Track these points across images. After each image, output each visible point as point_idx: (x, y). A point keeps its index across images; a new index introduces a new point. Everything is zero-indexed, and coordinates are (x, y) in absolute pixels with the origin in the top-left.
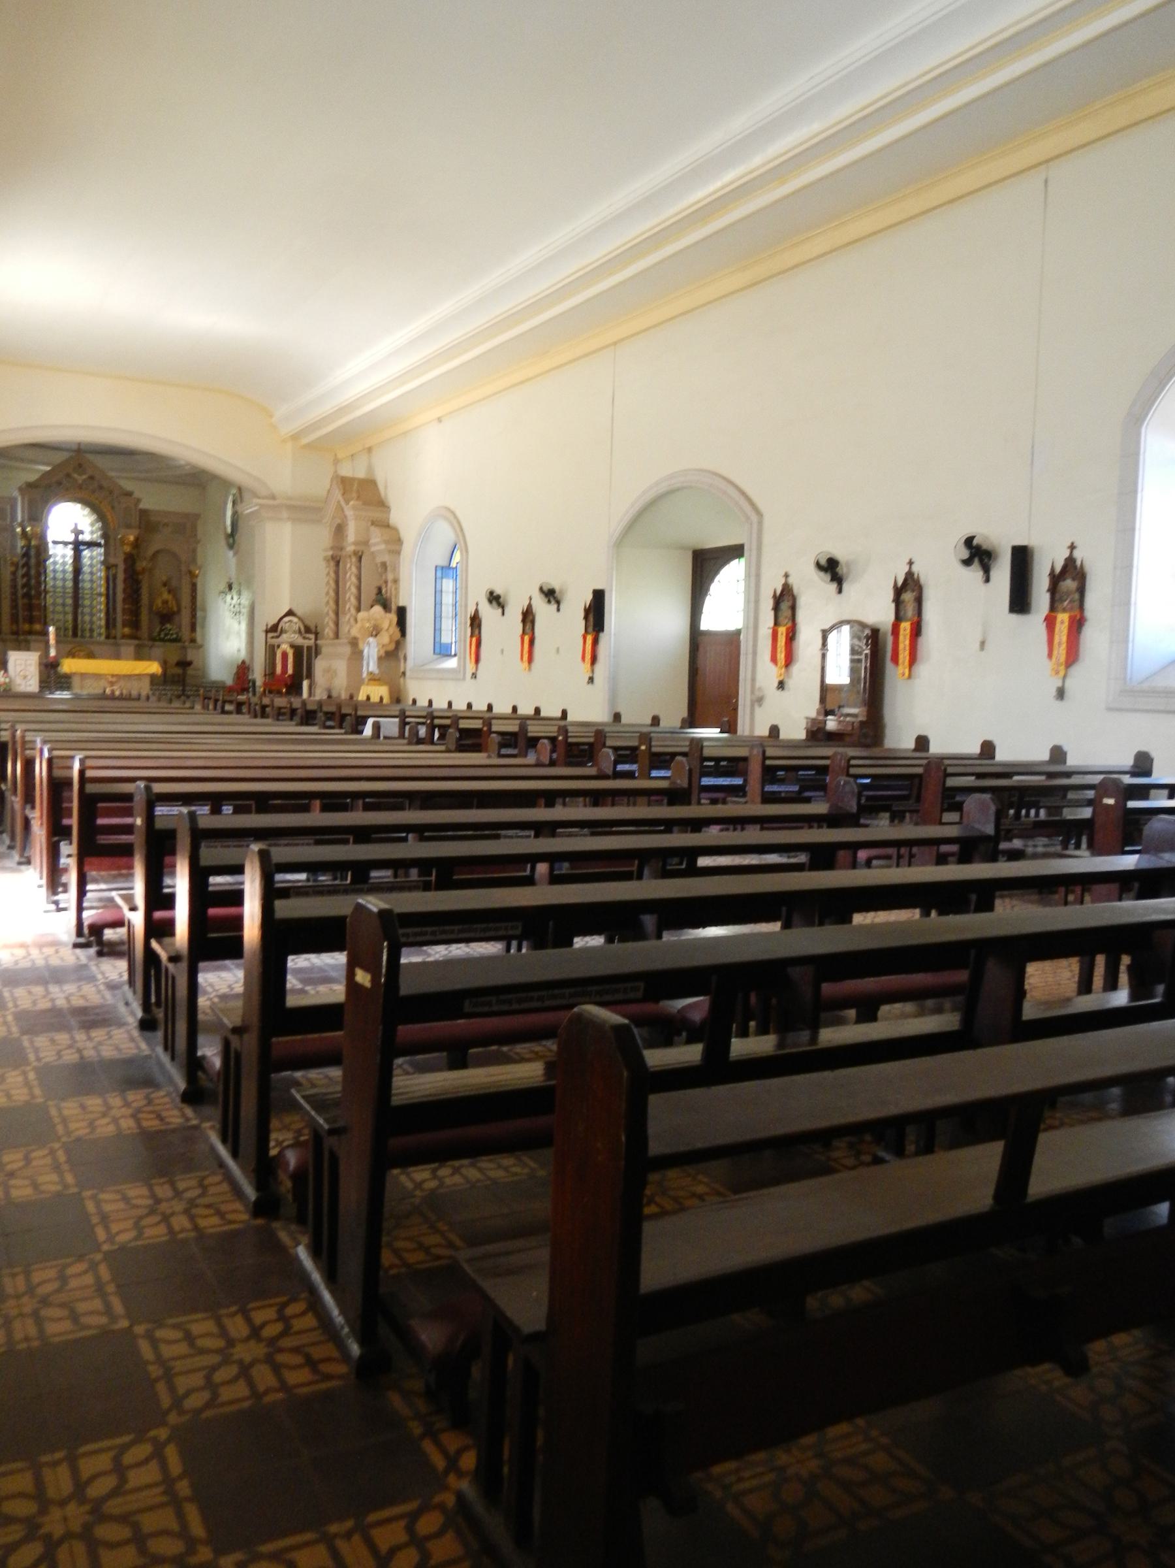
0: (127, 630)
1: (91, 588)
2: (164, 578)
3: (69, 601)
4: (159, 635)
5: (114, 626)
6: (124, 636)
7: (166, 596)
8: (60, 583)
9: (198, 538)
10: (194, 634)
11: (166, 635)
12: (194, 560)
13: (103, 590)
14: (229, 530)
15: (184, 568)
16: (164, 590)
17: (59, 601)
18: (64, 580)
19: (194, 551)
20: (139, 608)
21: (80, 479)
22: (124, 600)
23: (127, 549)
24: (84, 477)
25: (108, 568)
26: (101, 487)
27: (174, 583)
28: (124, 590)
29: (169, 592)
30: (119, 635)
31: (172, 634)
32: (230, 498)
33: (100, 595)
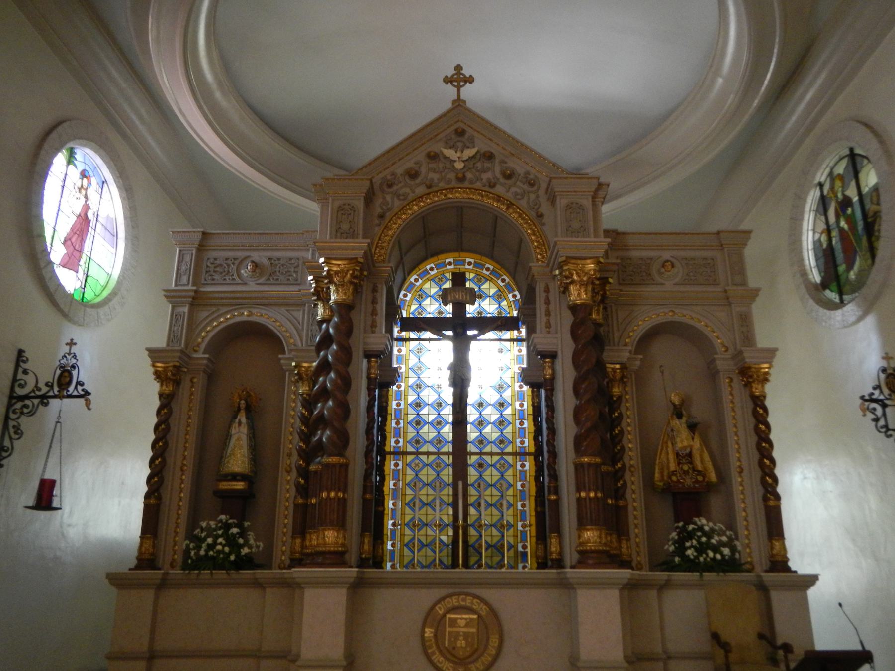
0: (590, 535)
1: (502, 441)
3: (447, 474)
4: (681, 549)
5: (557, 529)
6: (585, 558)
7: (684, 439)
8: (429, 433)
9: (752, 283)
11: (701, 549)
12: (748, 339)
13: (528, 444)
14: (816, 277)
15: (724, 364)
17: (427, 475)
18: (438, 423)
19: (746, 320)
20: (618, 475)
21: (457, 157)
22: (578, 443)
23: (578, 295)
24: (469, 153)
25: (535, 386)
26: (509, 176)
27: (700, 411)
28: (577, 413)
29: (692, 427)
30: (570, 556)
32: (813, 196)
33: (521, 454)
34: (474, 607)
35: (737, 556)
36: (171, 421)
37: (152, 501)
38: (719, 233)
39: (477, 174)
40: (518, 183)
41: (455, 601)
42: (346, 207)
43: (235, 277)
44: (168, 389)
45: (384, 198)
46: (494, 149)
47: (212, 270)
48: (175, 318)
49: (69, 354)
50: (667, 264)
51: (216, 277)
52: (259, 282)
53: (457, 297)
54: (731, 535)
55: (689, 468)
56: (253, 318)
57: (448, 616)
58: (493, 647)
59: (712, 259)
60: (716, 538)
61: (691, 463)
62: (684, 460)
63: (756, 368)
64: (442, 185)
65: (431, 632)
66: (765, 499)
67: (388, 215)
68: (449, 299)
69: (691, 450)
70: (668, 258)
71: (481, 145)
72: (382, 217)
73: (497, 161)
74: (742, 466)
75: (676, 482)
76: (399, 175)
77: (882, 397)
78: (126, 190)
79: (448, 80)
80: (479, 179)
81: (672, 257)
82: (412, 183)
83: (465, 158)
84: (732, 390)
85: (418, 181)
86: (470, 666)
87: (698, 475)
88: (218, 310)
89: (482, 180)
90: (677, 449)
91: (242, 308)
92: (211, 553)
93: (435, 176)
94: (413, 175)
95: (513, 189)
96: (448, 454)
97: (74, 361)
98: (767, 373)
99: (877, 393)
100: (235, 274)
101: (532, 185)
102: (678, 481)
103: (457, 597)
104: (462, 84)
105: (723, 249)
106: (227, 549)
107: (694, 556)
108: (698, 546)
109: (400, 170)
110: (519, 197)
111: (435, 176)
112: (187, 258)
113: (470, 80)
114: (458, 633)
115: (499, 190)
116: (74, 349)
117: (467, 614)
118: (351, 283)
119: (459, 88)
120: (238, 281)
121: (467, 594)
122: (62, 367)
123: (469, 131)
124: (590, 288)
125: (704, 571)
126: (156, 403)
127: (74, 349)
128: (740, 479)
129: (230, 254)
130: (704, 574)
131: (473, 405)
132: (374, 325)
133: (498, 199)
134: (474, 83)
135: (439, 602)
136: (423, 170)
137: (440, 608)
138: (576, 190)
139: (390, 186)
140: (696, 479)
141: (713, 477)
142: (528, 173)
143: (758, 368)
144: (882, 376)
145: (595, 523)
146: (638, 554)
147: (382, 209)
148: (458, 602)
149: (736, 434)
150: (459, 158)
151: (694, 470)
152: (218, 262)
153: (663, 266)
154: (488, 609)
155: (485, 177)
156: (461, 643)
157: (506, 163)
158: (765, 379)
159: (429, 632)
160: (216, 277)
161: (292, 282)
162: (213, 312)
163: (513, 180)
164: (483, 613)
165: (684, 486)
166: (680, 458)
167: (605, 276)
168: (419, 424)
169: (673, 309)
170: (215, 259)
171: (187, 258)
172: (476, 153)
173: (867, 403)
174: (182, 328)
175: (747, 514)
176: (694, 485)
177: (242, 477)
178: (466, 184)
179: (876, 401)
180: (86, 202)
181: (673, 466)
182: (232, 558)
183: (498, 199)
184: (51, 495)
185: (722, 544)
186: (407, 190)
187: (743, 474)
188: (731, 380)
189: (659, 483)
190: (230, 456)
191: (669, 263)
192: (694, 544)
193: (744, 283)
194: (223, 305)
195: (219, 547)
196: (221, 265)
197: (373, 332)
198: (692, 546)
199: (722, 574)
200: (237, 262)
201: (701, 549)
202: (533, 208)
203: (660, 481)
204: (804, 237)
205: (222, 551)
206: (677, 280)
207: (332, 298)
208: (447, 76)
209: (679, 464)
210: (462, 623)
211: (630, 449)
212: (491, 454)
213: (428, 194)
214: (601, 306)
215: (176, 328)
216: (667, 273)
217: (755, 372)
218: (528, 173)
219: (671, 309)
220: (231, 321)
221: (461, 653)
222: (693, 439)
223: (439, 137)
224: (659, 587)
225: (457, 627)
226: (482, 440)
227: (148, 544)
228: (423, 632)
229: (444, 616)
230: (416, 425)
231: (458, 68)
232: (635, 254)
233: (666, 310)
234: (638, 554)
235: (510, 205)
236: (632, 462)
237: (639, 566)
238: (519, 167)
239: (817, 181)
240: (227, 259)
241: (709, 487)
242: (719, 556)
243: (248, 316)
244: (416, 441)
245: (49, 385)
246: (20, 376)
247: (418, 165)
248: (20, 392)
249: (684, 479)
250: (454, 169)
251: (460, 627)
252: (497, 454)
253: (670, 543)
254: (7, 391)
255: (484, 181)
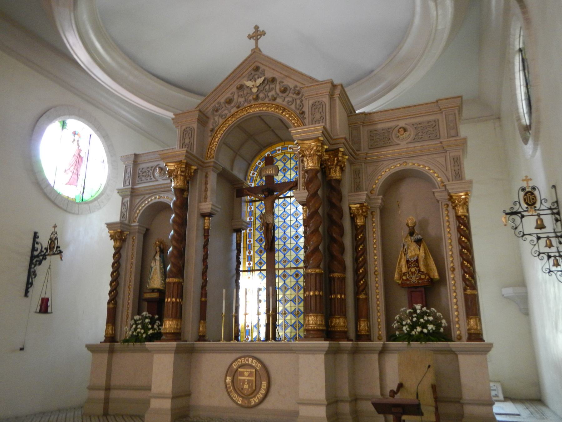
2: (411, 220)
7: (414, 251)
10: (472, 322)
11: (413, 326)
12: (459, 175)
14: (526, 120)
16: (410, 241)
24: (259, 81)
26: (284, 90)
27: (432, 231)
29: (418, 242)
31: (424, 326)
34: (253, 364)
35: (442, 330)
36: (120, 261)
37: (111, 306)
38: (437, 101)
39: (266, 93)
40: (290, 95)
41: (242, 361)
42: (188, 129)
43: (152, 177)
44: (118, 244)
45: (214, 119)
46: (276, 75)
47: (141, 175)
48: (123, 204)
49: (54, 232)
50: (400, 130)
51: (143, 179)
52: (164, 178)
53: (267, 172)
54: (440, 316)
55: (416, 270)
56: (162, 200)
57: (239, 370)
58: (264, 389)
59: (435, 121)
60: (426, 318)
61: (418, 266)
62: (412, 265)
63: (457, 196)
64: (246, 104)
65: (230, 379)
66: (465, 290)
67: (216, 129)
68: (263, 174)
69: (418, 257)
70: (403, 125)
71: (269, 74)
72: (212, 130)
73: (278, 83)
74: (454, 267)
75: (406, 280)
76: (222, 103)
77: (520, 210)
78: (104, 137)
79: (250, 37)
80: (267, 96)
81: (405, 124)
82: (229, 107)
83: (258, 85)
84: (448, 213)
85: (233, 105)
86: (251, 400)
87: (422, 274)
88: (144, 197)
89: (268, 97)
90: (408, 257)
91: (155, 195)
92: (135, 333)
93: (241, 100)
94: (229, 101)
95: (287, 99)
96: (279, 269)
97: (56, 235)
98: (465, 199)
99: (516, 208)
100: (152, 176)
101: (298, 94)
102: (407, 280)
103: (244, 358)
104: (259, 37)
105: (442, 113)
106: (142, 331)
107: (407, 331)
108: (411, 324)
109: (223, 101)
110: (290, 103)
111: (241, 100)
112: (129, 170)
113: (264, 33)
114: (244, 380)
115: (279, 101)
116: (56, 229)
117: (250, 369)
118: (181, 175)
119: (257, 40)
120: (154, 179)
121: (249, 357)
122: (51, 239)
123: (262, 67)
124: (316, 158)
125: (412, 341)
126: (113, 251)
127: (56, 229)
128: (452, 276)
129: (150, 165)
130: (411, 343)
131: (301, 237)
132: (206, 198)
133: (277, 107)
134: (266, 35)
135: (234, 362)
136: (236, 97)
137: (235, 365)
138: (318, 93)
139: (217, 111)
140: (420, 277)
141: (436, 275)
142: (296, 86)
143: (459, 196)
144: (522, 194)
145: (316, 312)
146: (379, 329)
147: (213, 125)
148: (245, 361)
149: (451, 244)
150: (253, 85)
151: (419, 271)
152: (144, 170)
153: (399, 132)
154: (261, 366)
155: (270, 94)
156: (246, 386)
157: (283, 82)
158: (465, 203)
159: (229, 379)
160: (143, 179)
161: (149, 180)
162: (143, 198)
163: (287, 93)
164: (258, 368)
165: (411, 282)
166: (410, 263)
167: (338, 147)
168: (262, 252)
169: (406, 161)
170: (143, 169)
171: (129, 170)
172: (264, 80)
173: (508, 216)
174: (127, 209)
175: (457, 300)
176: (418, 282)
177: (159, 290)
178: (260, 101)
179: (516, 213)
180: (78, 148)
181: (404, 269)
182: (144, 336)
183: (277, 107)
184: (47, 307)
185: (428, 322)
186: (226, 112)
187: (455, 272)
188: (448, 205)
189: (398, 281)
190: (151, 279)
191: (402, 129)
192: (408, 323)
193: (457, 135)
194: (147, 194)
195: (139, 330)
196: (146, 172)
197: (206, 202)
198: (407, 324)
199: (423, 343)
200: (153, 169)
201: (413, 326)
202: (299, 109)
203: (400, 280)
204: (518, 92)
205: (140, 332)
206: (409, 140)
207: (173, 185)
208: (249, 35)
209: (408, 268)
210: (246, 374)
211: (376, 260)
212: (291, 268)
213: (237, 112)
214: (338, 168)
215: (124, 210)
216: (402, 136)
217: (456, 199)
218: (296, 86)
219: (404, 161)
220: (150, 203)
221: (246, 392)
222: (419, 249)
223: (244, 75)
224: (378, 352)
225: (243, 376)
226: (298, 260)
227: (110, 328)
228: (226, 379)
229: (237, 370)
230: (260, 253)
231: (256, 28)
232: (380, 126)
233: (401, 162)
234: (379, 329)
235: (284, 110)
236: (376, 268)
237: (380, 338)
238: (291, 84)
239: (517, 48)
240: (148, 168)
241: (432, 281)
242: (425, 331)
243: (159, 198)
244: (260, 262)
245: (46, 249)
246: (36, 246)
247: (233, 95)
248: (36, 253)
249: (411, 278)
250: (252, 93)
251: (245, 376)
252: (294, 268)
253: (395, 322)
254: (29, 254)
255: (270, 97)
